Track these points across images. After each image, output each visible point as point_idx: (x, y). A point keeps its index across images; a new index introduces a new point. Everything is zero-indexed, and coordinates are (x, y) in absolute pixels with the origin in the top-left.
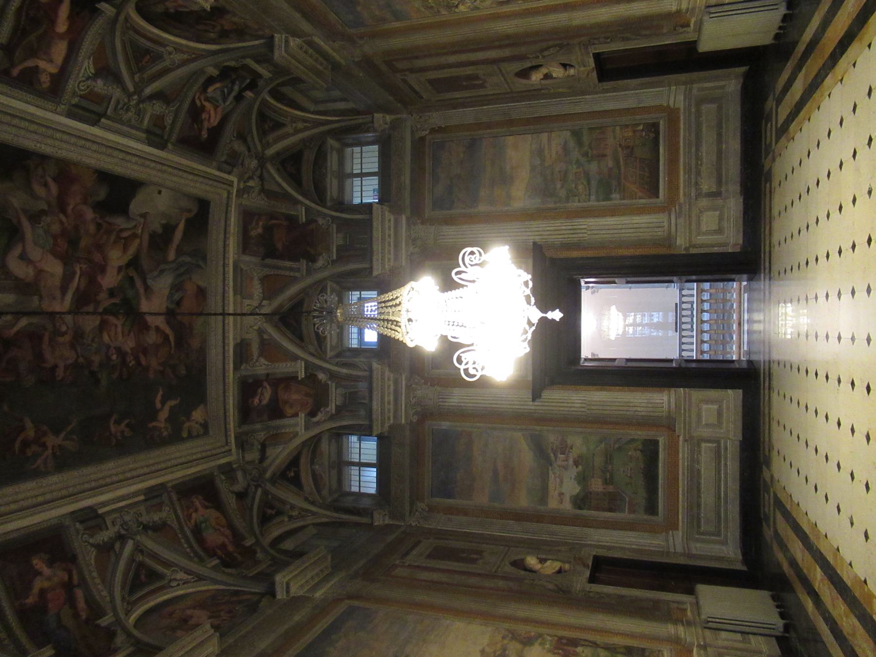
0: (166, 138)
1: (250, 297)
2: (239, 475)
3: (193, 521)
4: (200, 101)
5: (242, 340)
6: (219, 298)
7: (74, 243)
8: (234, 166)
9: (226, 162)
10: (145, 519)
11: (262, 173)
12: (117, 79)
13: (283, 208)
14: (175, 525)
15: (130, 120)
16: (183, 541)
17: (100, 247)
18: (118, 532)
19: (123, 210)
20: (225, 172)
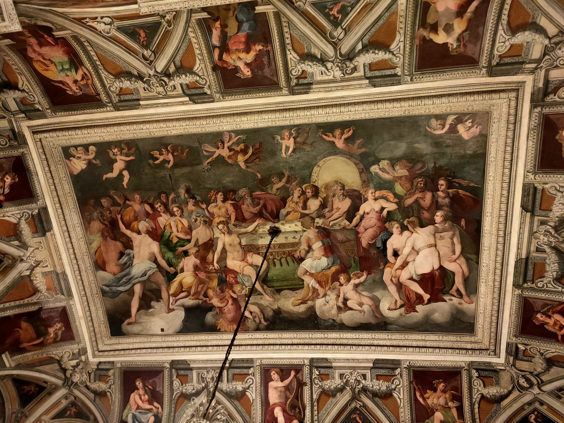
0: (174, 370)
1: (45, 274)
2: (13, 106)
3: (80, 72)
4: (156, 407)
5: (44, 235)
6: (82, 267)
7: (222, 282)
8: (98, 369)
9: (108, 370)
10: (140, 85)
11: (65, 374)
12: (229, 395)
13: (30, 356)
14: (104, 74)
15: (208, 372)
16: (95, 58)
17: (201, 282)
18: (170, 80)
19: (188, 310)
20: (105, 362)
